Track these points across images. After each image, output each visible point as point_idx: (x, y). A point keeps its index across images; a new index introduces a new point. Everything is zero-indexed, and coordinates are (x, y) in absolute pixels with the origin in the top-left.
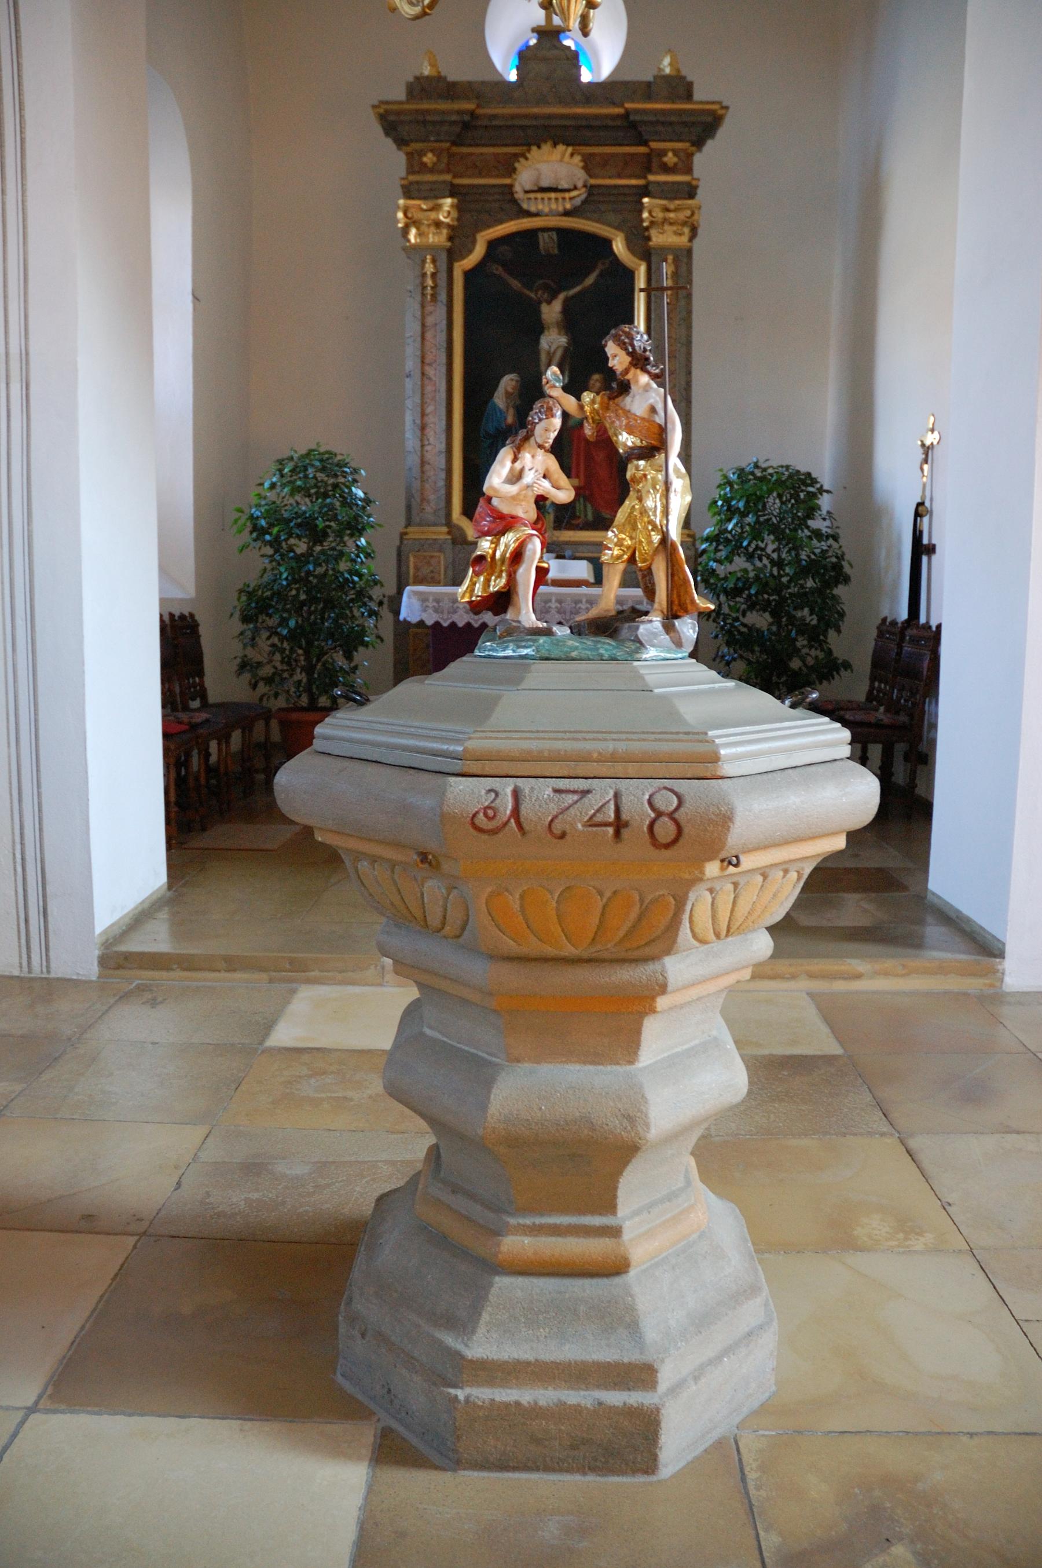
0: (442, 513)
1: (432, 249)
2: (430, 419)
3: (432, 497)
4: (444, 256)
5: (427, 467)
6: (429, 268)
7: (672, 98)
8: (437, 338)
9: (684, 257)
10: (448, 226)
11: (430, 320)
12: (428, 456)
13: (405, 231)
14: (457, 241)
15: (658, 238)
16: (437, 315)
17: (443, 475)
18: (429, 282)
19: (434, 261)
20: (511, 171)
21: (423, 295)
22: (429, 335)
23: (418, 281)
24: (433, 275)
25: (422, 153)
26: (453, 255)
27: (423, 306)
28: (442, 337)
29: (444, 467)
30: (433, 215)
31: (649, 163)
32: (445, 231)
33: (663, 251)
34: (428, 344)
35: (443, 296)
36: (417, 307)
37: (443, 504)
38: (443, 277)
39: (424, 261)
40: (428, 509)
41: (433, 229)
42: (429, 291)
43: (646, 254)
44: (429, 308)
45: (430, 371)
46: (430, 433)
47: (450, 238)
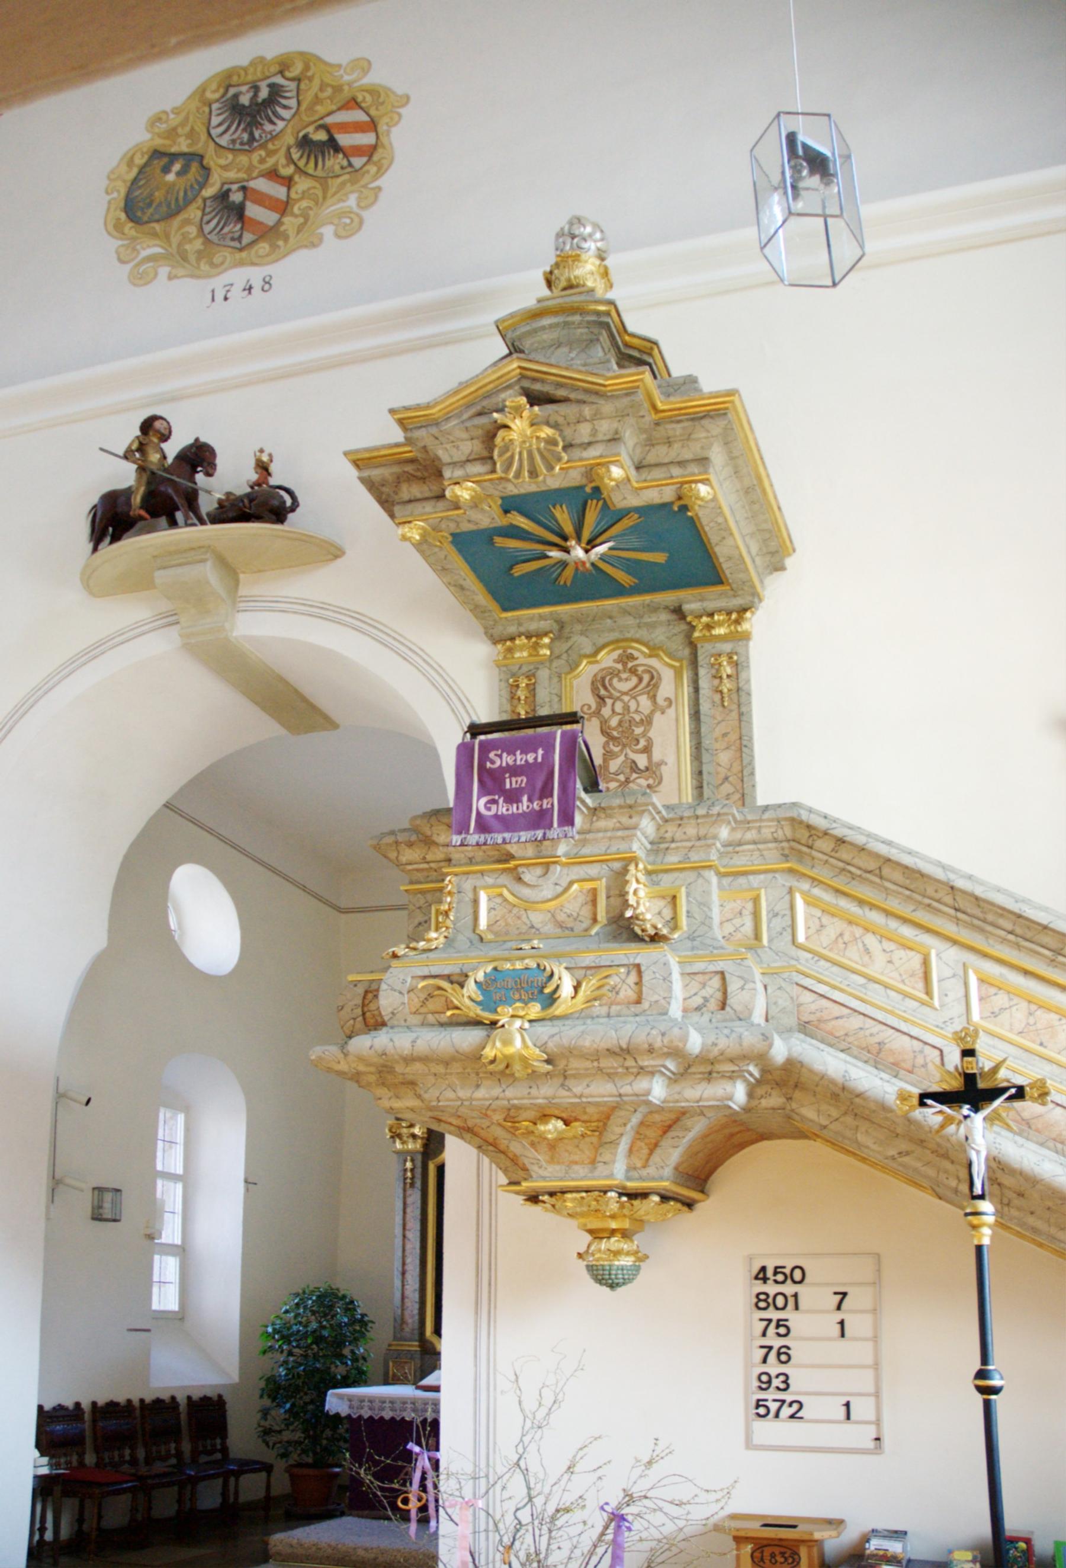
0: (416, 1332)
2: (409, 1267)
3: (410, 1321)
4: (419, 1158)
5: (406, 1300)
6: (409, 1165)
8: (414, 1212)
10: (422, 1138)
11: (409, 1200)
12: (407, 1293)
14: (432, 1146)
16: (415, 1197)
17: (417, 1306)
18: (409, 1174)
19: (412, 1160)
21: (405, 1184)
22: (408, 1210)
23: (401, 1174)
24: (412, 1170)
27: (405, 1190)
28: (418, 1212)
29: (417, 1300)
30: (412, 1130)
32: (419, 1141)
34: (408, 1216)
35: (418, 1184)
36: (401, 1191)
37: (416, 1326)
38: (419, 1171)
39: (405, 1161)
40: (407, 1329)
41: (411, 1140)
42: (408, 1181)
44: (409, 1192)
45: (409, 1235)
46: (408, 1276)
47: (426, 1146)
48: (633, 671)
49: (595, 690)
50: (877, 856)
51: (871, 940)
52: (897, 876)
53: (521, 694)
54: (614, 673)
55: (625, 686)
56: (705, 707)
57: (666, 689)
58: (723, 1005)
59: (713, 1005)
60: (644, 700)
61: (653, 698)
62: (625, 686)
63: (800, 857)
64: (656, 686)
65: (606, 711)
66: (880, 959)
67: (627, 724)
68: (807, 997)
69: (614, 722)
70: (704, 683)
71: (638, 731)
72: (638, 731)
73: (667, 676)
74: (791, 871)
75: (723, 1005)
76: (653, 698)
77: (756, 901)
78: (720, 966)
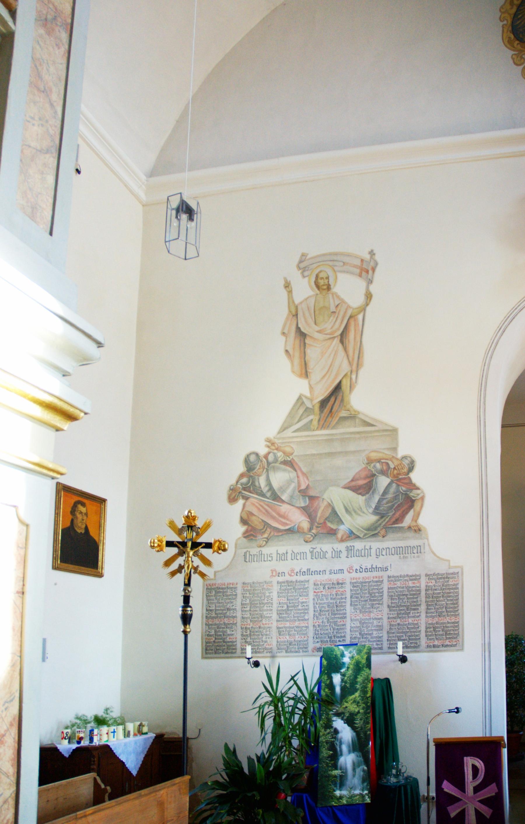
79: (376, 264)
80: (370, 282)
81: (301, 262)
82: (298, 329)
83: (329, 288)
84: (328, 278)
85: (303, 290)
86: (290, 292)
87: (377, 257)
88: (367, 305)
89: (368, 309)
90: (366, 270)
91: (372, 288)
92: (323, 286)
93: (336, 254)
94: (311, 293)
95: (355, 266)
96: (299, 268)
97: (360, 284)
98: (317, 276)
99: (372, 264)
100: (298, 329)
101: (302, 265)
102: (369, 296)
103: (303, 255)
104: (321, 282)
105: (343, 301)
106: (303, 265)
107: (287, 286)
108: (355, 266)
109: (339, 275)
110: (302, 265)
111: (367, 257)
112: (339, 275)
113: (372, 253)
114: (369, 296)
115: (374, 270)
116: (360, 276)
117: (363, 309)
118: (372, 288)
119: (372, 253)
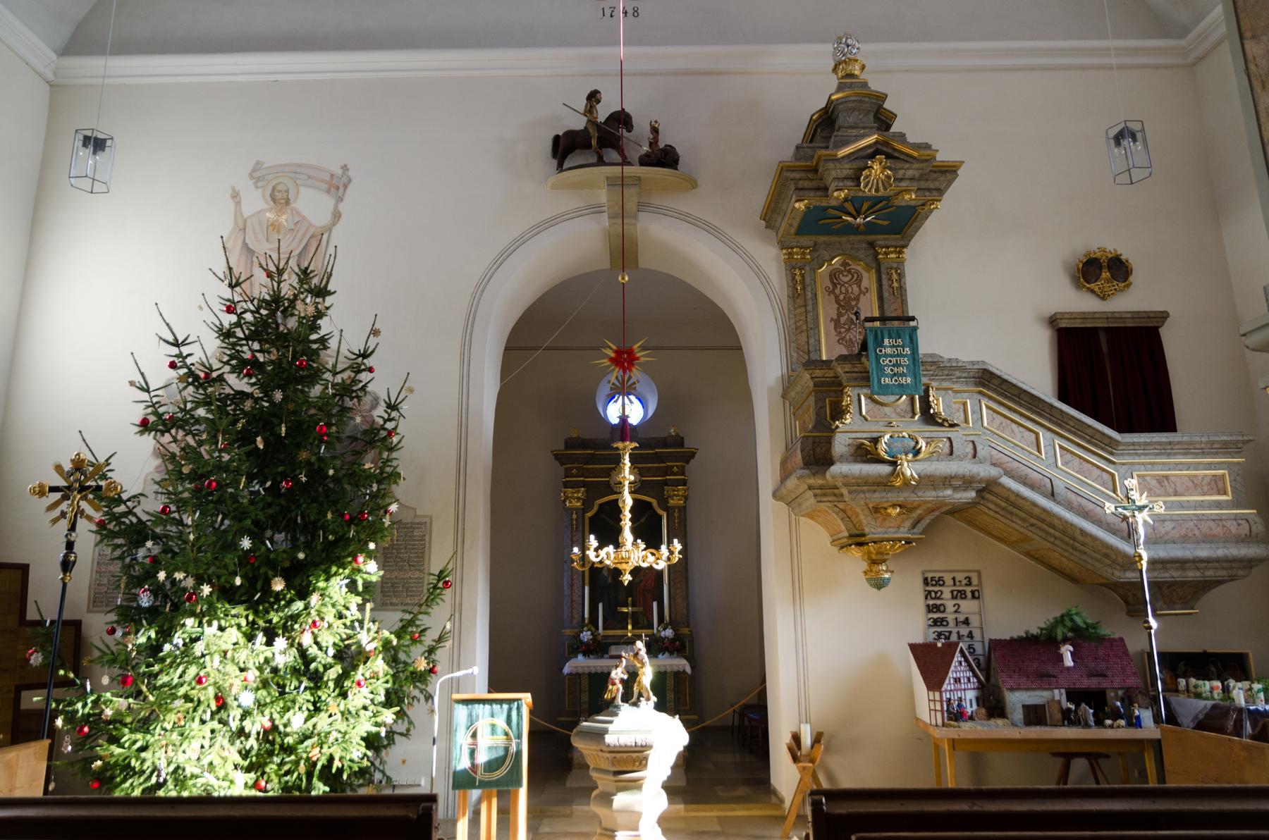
1: (576, 509)
7: (674, 446)
9: (683, 510)
13: (564, 501)
15: (672, 502)
20: (609, 476)
25: (572, 469)
26: (584, 511)
31: (668, 471)
33: (674, 508)
43: (666, 509)
48: (849, 272)
49: (831, 280)
50: (1020, 389)
51: (1014, 426)
52: (1027, 398)
53: (798, 278)
54: (841, 272)
55: (846, 279)
56: (886, 294)
57: (865, 283)
58: (975, 456)
59: (970, 456)
60: (855, 287)
61: (859, 287)
62: (846, 279)
63: (983, 386)
64: (861, 281)
65: (837, 291)
66: (1019, 435)
67: (848, 299)
68: (994, 452)
69: (842, 297)
70: (885, 282)
71: (854, 303)
72: (854, 303)
73: (865, 274)
74: (980, 393)
75: (975, 456)
76: (859, 287)
77: (965, 404)
78: (972, 438)
79: (350, 181)
80: (340, 199)
81: (254, 170)
82: (245, 245)
83: (287, 202)
84: (287, 191)
85: (255, 202)
86: (238, 203)
87: (351, 173)
88: (334, 224)
89: (335, 230)
90: (337, 186)
91: (341, 207)
92: (280, 200)
93: (300, 166)
94: (264, 206)
95: (322, 181)
96: (251, 177)
97: (328, 202)
98: (274, 188)
99: (344, 180)
100: (245, 245)
101: (256, 174)
102: (337, 216)
103: (258, 163)
104: (279, 195)
105: (304, 218)
106: (257, 175)
107: (235, 195)
108: (322, 181)
109: (302, 190)
110: (256, 174)
111: (340, 172)
112: (302, 190)
113: (345, 168)
114: (337, 216)
115: (346, 187)
116: (328, 192)
117: (329, 229)
118: (341, 207)
119: (345, 168)
